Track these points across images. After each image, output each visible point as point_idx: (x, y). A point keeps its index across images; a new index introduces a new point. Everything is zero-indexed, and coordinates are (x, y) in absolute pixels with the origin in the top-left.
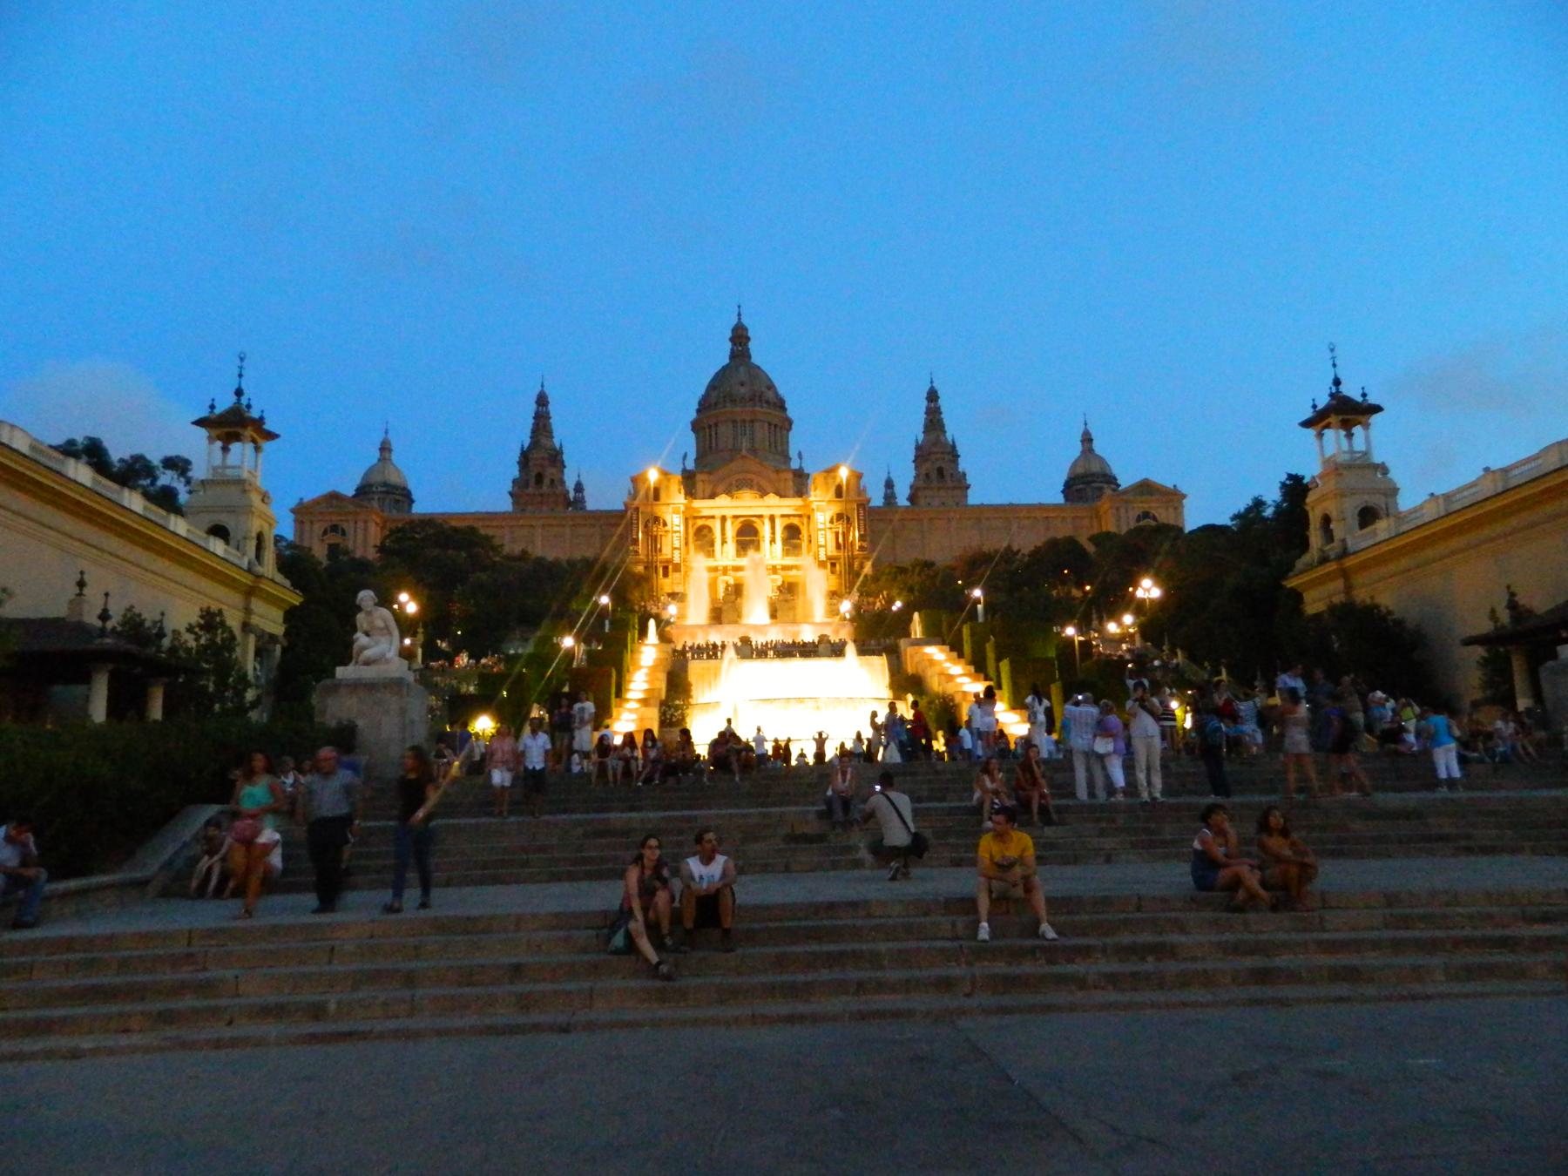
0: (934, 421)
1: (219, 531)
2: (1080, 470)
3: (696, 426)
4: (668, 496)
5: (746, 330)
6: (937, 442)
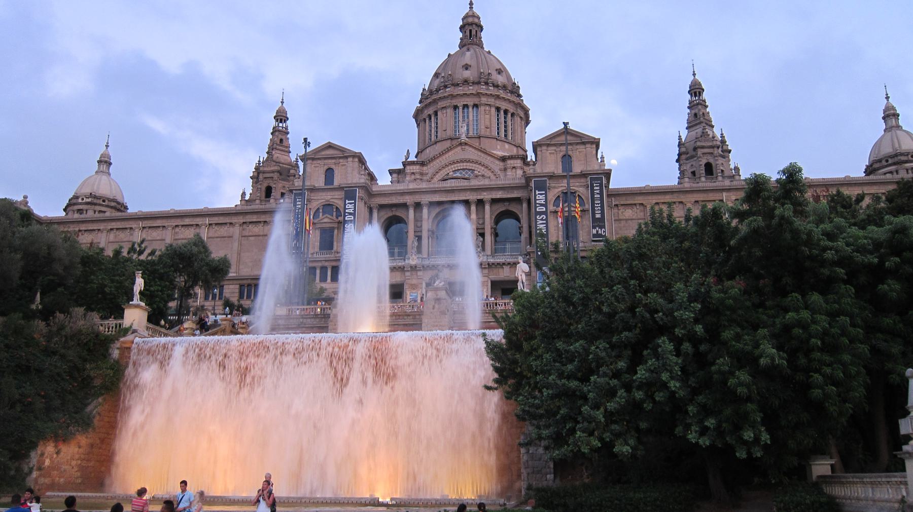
0: (698, 116)
2: (887, 150)
5: (479, 18)
6: (704, 134)
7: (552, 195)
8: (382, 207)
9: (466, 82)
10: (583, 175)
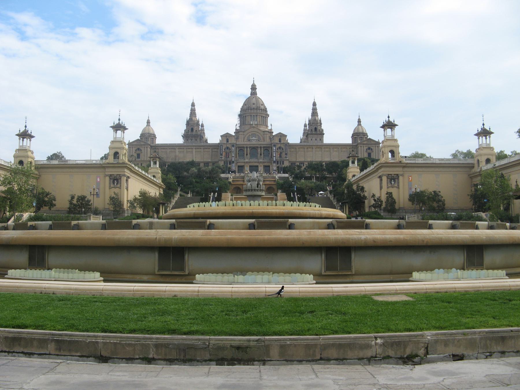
0: (314, 113)
1: (154, 176)
2: (356, 131)
3: (240, 116)
6: (315, 119)
7: (277, 147)
8: (238, 147)
9: (254, 109)
10: (283, 143)
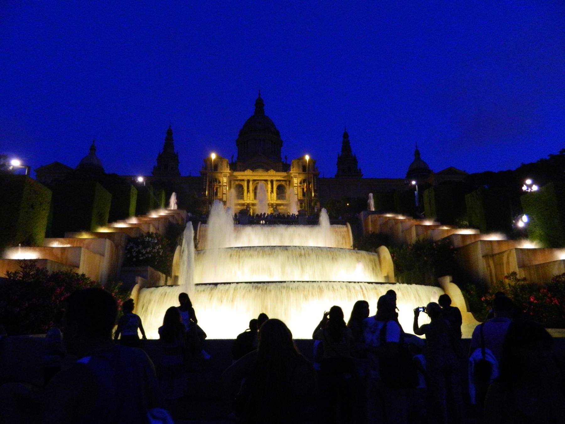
0: (346, 146)
4: (221, 170)
